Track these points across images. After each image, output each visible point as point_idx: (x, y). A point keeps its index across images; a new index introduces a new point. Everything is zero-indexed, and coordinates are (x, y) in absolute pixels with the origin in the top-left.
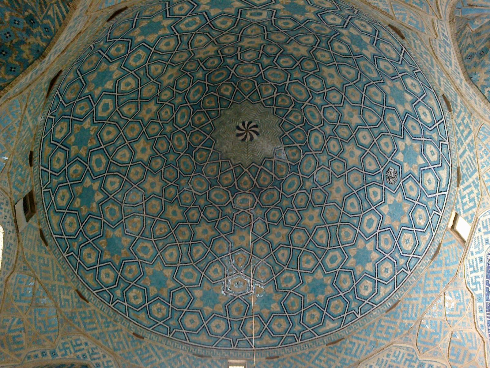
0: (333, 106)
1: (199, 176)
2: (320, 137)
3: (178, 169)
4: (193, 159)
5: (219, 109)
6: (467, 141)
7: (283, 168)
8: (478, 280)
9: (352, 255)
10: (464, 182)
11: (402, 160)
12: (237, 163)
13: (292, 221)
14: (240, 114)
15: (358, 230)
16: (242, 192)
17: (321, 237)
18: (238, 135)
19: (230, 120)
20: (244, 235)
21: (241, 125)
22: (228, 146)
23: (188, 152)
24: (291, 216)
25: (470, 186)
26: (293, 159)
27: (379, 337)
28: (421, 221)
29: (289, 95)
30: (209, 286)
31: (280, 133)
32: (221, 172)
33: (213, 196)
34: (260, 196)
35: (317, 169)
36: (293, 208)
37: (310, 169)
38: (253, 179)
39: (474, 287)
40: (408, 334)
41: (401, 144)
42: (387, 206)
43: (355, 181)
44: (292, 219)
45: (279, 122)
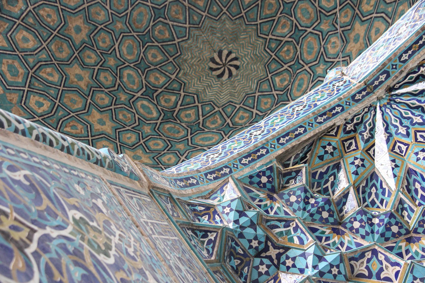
1: (138, 43)
3: (130, 9)
4: (151, 24)
5: (225, 10)
7: (217, 122)
12: (182, 79)
13: (166, 161)
14: (235, 39)
16: (156, 103)
18: (213, 60)
19: (222, 34)
20: (107, 124)
21: (225, 52)
22: (192, 58)
23: (155, 10)
26: (236, 122)
29: (298, 47)
30: (14, 101)
31: (252, 90)
32: (160, 68)
33: (126, 72)
34: (166, 121)
38: (178, 106)
45: (262, 77)
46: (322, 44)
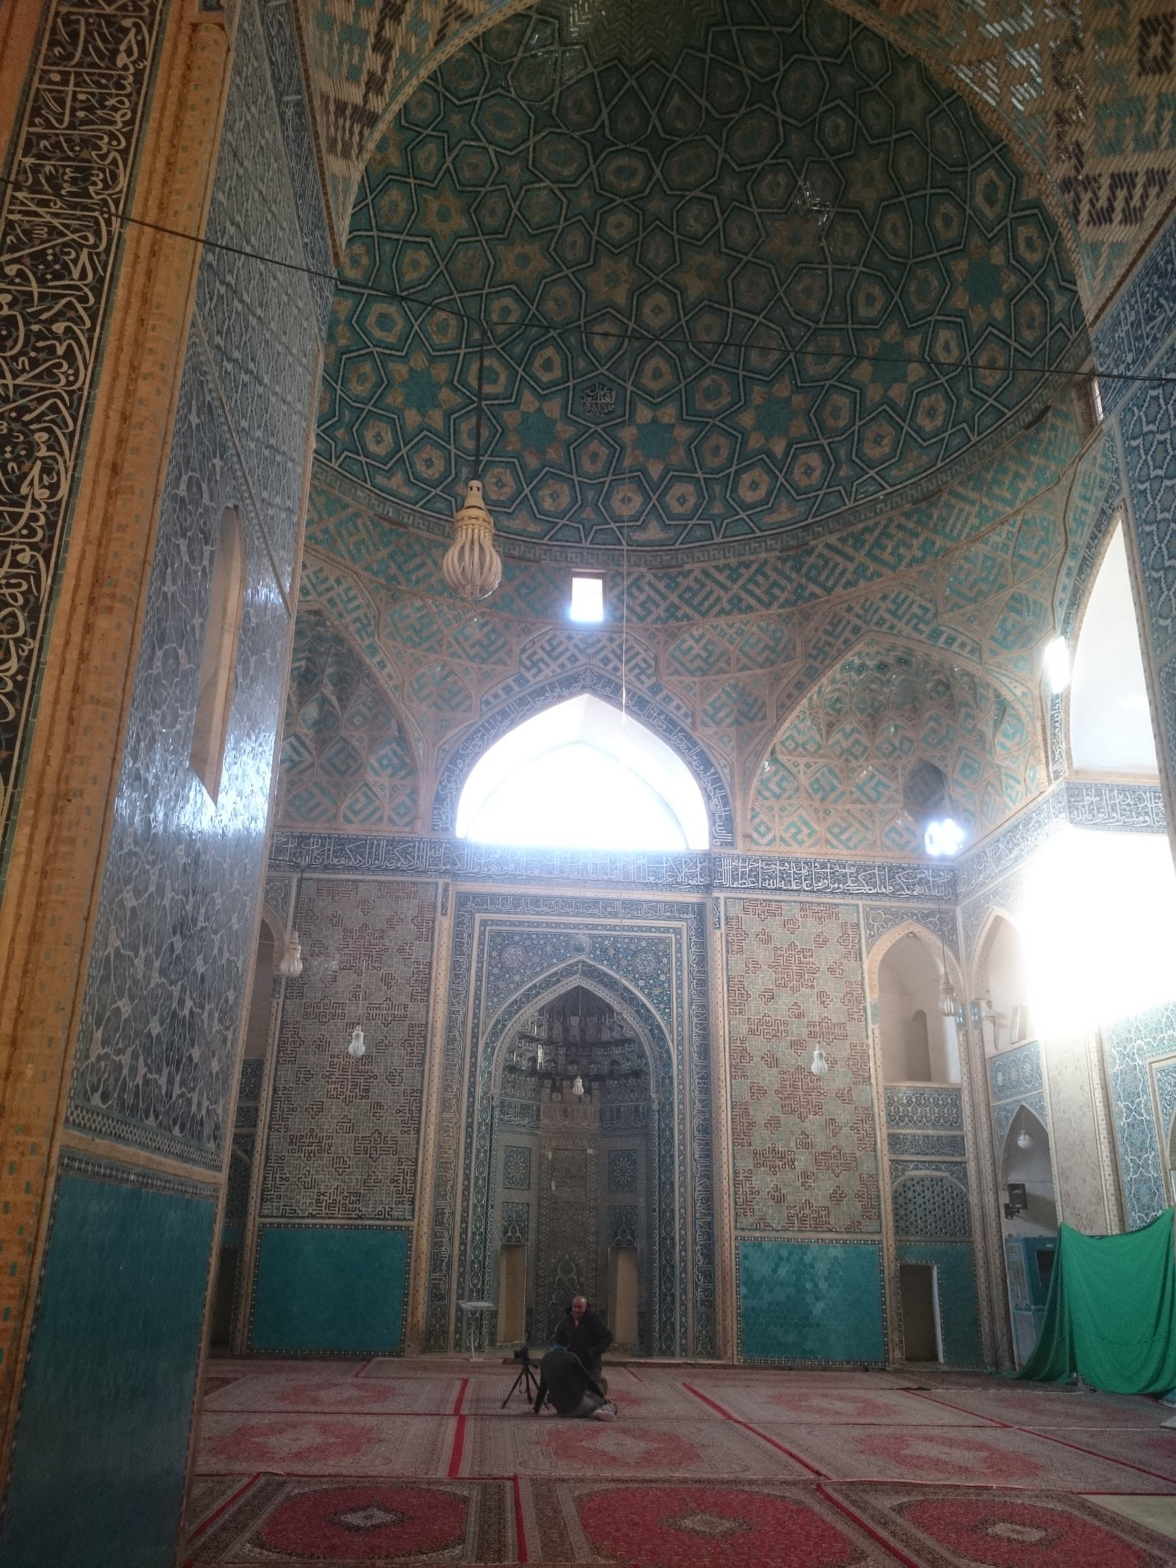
0: (720, 224)
2: (635, 184)
6: (744, 595)
8: (541, 665)
9: (412, 364)
10: (660, 579)
11: (638, 421)
13: (422, 163)
15: (462, 352)
17: (415, 264)
24: (431, 154)
25: (664, 598)
27: (341, 536)
28: (549, 500)
35: (555, 187)
36: (450, 151)
37: (552, 167)
39: (528, 663)
40: (383, 586)
41: (668, 414)
42: (537, 405)
43: (556, 301)
44: (428, 159)
46: (768, 161)
